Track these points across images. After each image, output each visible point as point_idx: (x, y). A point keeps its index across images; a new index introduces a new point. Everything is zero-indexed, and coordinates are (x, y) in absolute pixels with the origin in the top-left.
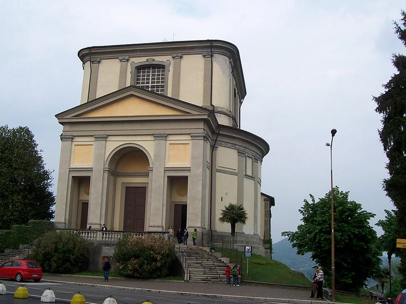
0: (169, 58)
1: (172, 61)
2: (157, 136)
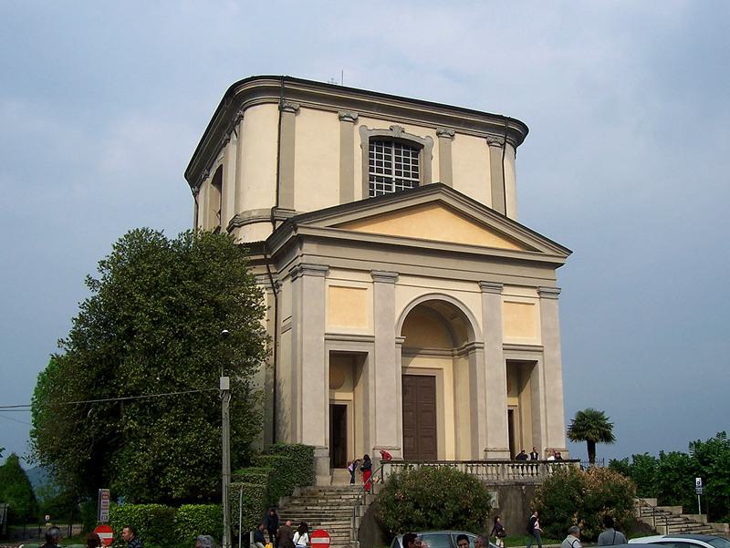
0: (432, 133)
1: (436, 140)
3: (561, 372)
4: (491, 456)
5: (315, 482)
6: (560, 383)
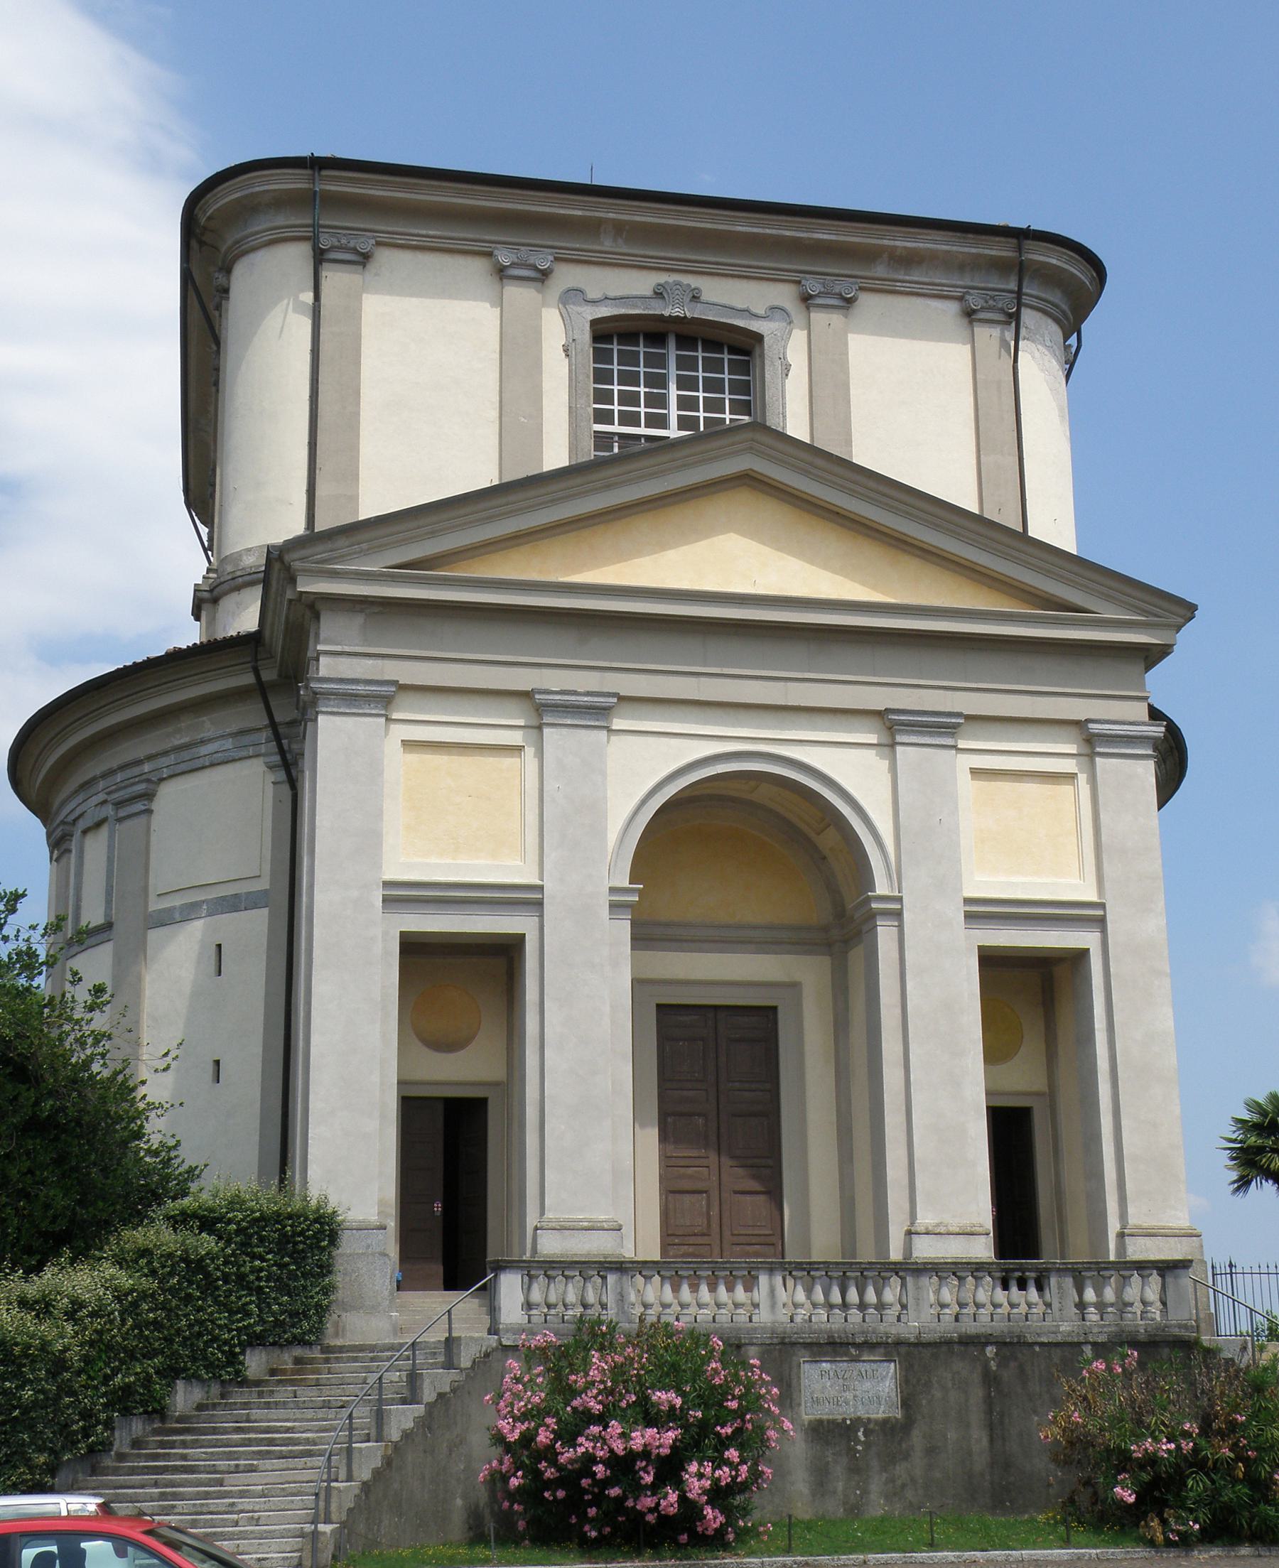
2: (894, 727)
3: (1167, 982)
4: (925, 1250)
5: (318, 1330)
6: (1164, 1018)
